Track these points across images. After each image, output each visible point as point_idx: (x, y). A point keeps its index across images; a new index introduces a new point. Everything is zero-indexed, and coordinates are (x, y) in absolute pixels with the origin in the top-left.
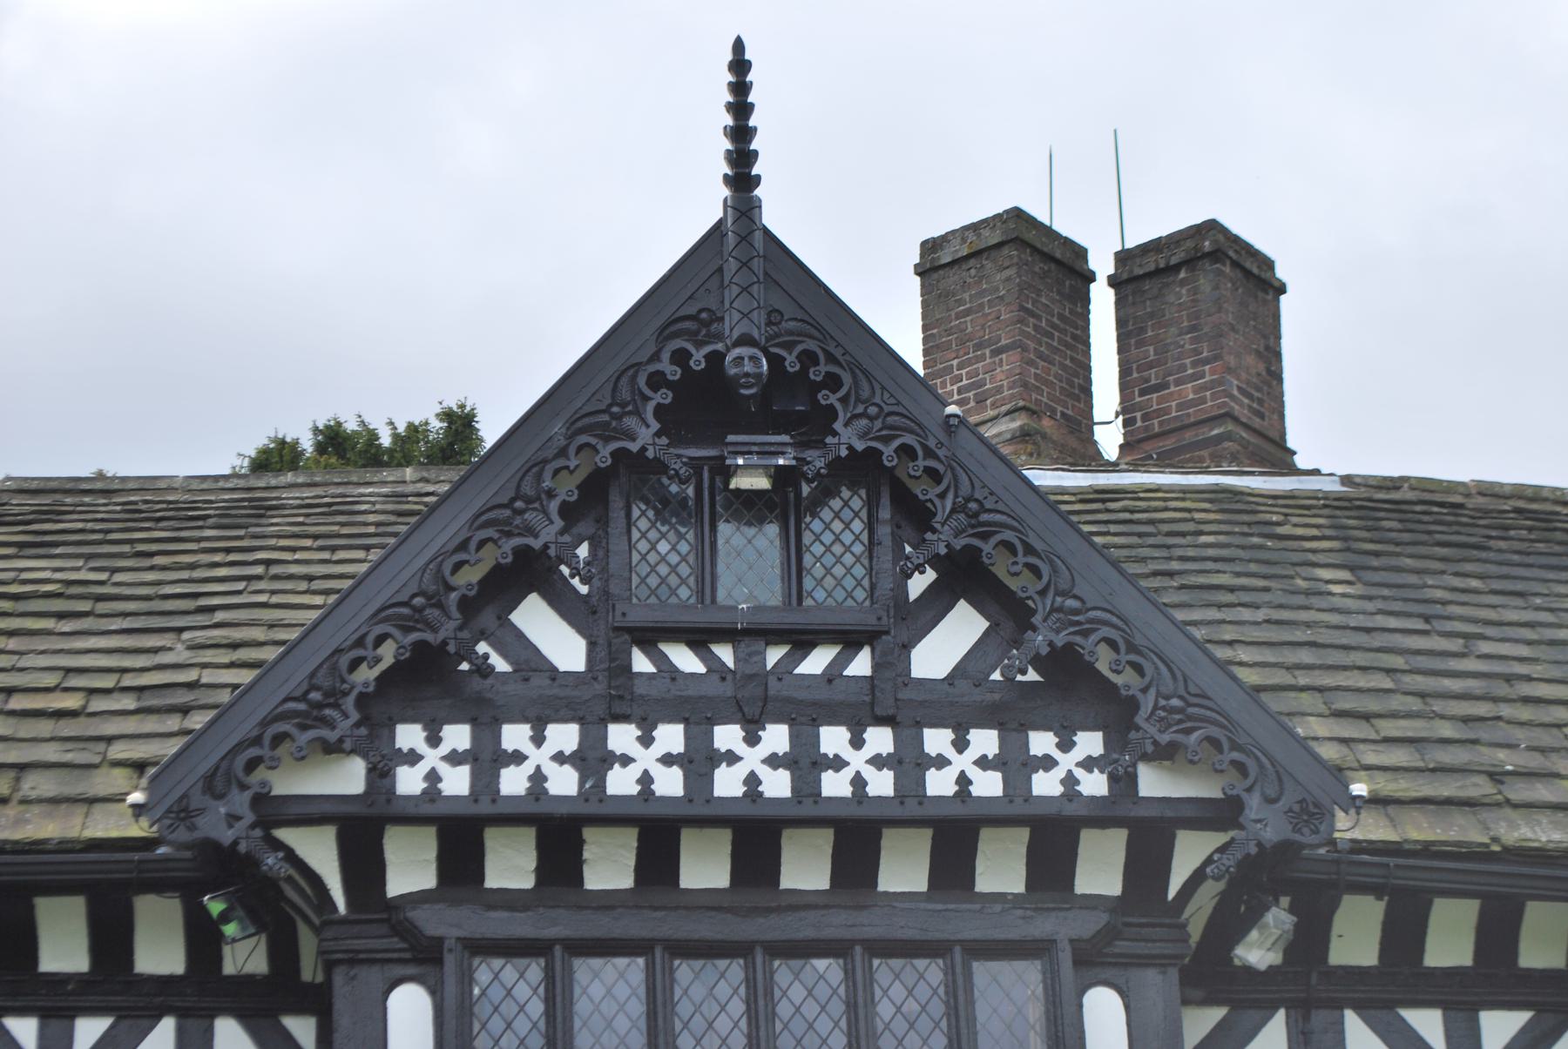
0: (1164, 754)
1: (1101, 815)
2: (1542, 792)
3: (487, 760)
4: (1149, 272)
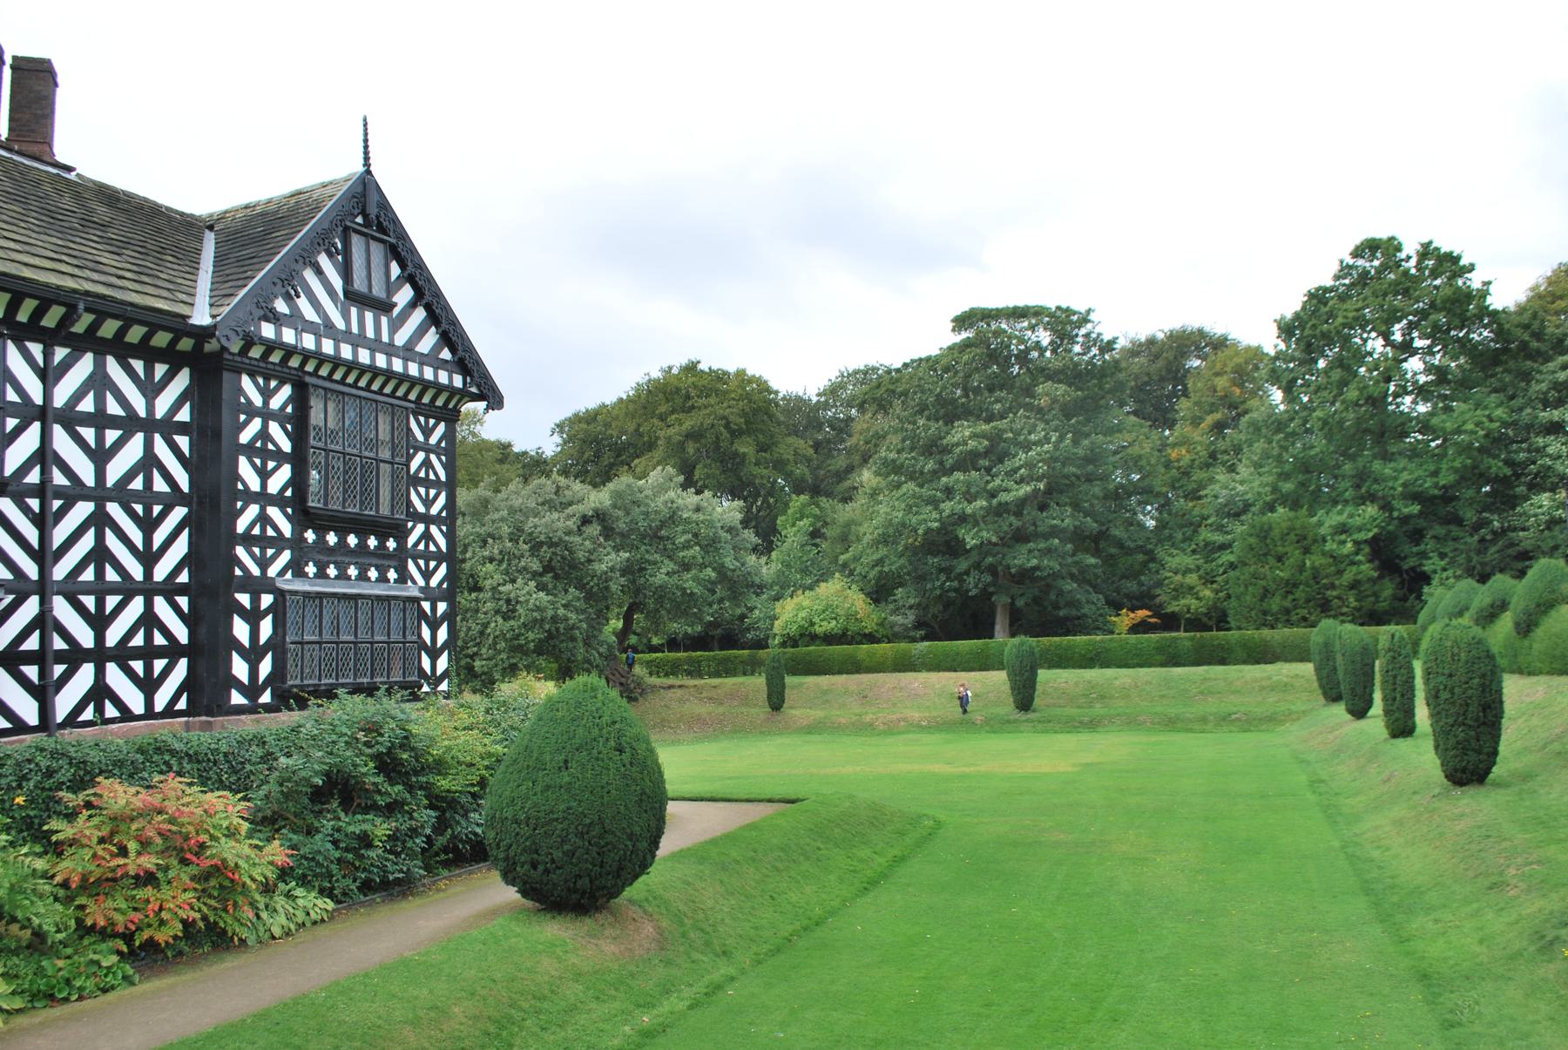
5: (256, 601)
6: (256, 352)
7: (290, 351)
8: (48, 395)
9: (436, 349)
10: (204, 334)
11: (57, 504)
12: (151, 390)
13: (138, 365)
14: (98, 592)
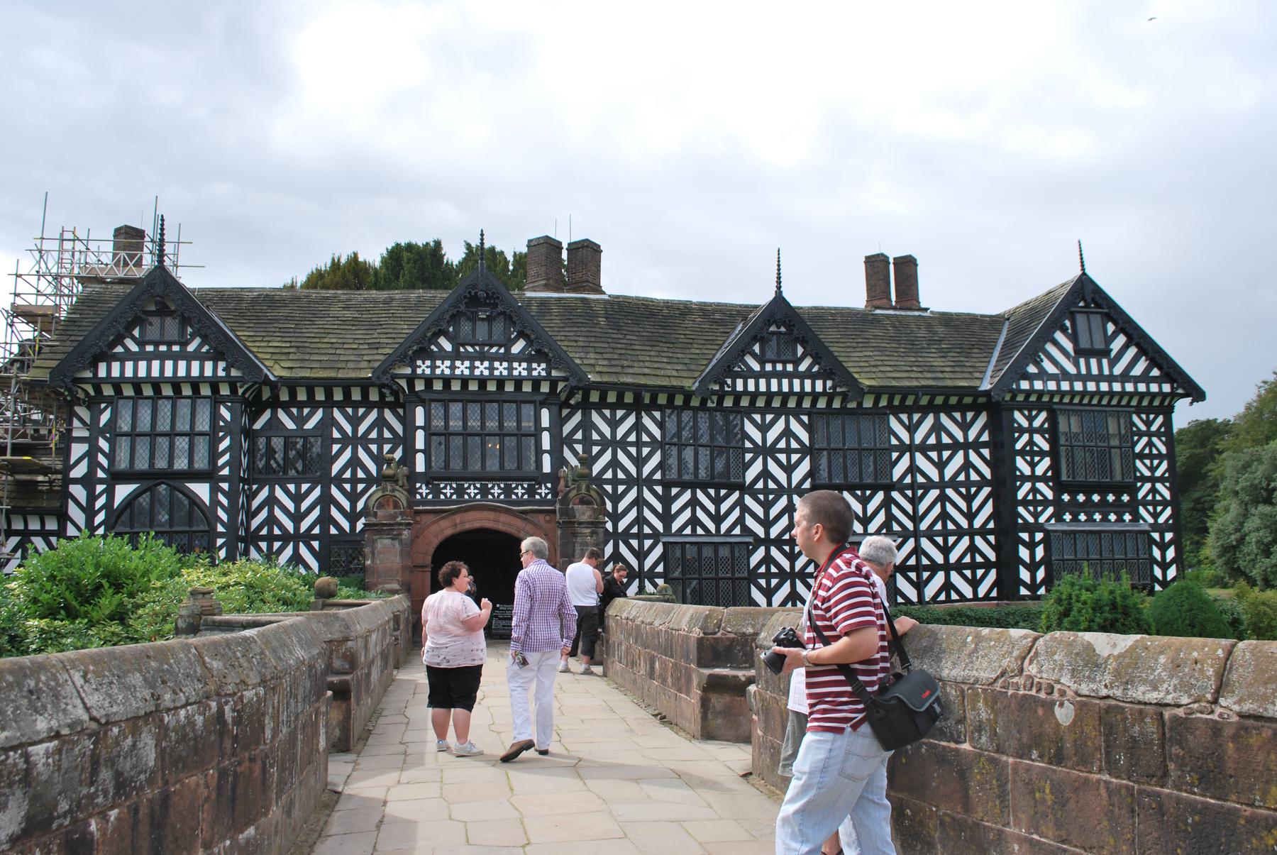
0: (556, 368)
1: (545, 379)
2: (631, 371)
3: (433, 367)
4: (573, 248)
5: (1032, 537)
6: (1020, 398)
7: (1041, 394)
8: (912, 439)
9: (1148, 370)
10: (987, 394)
11: (920, 492)
12: (965, 427)
13: (957, 415)
14: (944, 534)
